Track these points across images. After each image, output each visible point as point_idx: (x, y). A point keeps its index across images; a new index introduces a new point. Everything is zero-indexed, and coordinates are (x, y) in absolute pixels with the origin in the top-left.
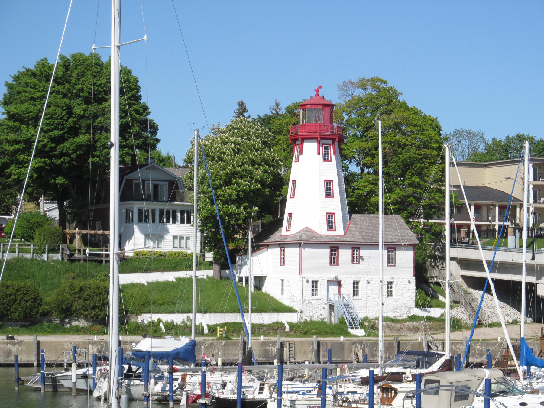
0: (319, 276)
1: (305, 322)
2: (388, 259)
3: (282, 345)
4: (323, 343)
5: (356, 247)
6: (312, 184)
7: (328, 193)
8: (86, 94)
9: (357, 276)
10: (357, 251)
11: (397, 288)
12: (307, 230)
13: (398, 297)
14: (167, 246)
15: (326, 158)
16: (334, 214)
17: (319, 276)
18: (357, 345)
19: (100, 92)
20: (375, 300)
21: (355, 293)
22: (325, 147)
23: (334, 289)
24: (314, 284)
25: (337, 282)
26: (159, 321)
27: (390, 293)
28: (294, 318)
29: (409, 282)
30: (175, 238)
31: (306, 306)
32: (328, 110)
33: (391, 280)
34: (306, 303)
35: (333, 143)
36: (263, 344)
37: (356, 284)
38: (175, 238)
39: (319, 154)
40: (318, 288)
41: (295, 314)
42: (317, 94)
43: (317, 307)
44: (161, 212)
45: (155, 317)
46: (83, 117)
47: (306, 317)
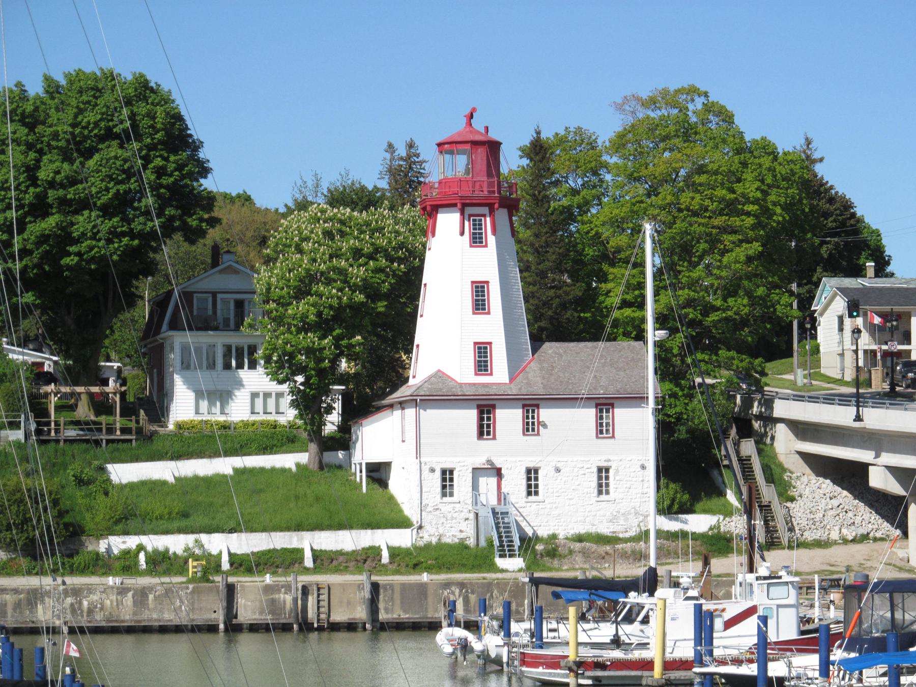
0: (458, 459)
1: (428, 546)
2: (480, 427)
3: (305, 591)
4: (385, 586)
5: (530, 405)
6: (462, 289)
7: (480, 305)
8: (62, 144)
9: (533, 459)
10: (533, 411)
11: (617, 478)
12: (440, 375)
14: (239, 410)
15: (477, 240)
18: (453, 588)
19: (86, 138)
20: (571, 502)
21: (532, 489)
22: (474, 220)
23: (488, 484)
24: (447, 476)
25: (495, 471)
26: (141, 548)
27: (602, 487)
28: (402, 538)
29: (643, 467)
30: (254, 395)
31: (430, 517)
32: (481, 152)
34: (429, 509)
35: (492, 213)
36: (268, 589)
37: (532, 474)
38: (254, 395)
39: (462, 233)
40: (455, 483)
41: (408, 531)
42: (469, 124)
43: (452, 518)
44: (228, 348)
45: (132, 542)
46: (52, 184)
47: (429, 536)
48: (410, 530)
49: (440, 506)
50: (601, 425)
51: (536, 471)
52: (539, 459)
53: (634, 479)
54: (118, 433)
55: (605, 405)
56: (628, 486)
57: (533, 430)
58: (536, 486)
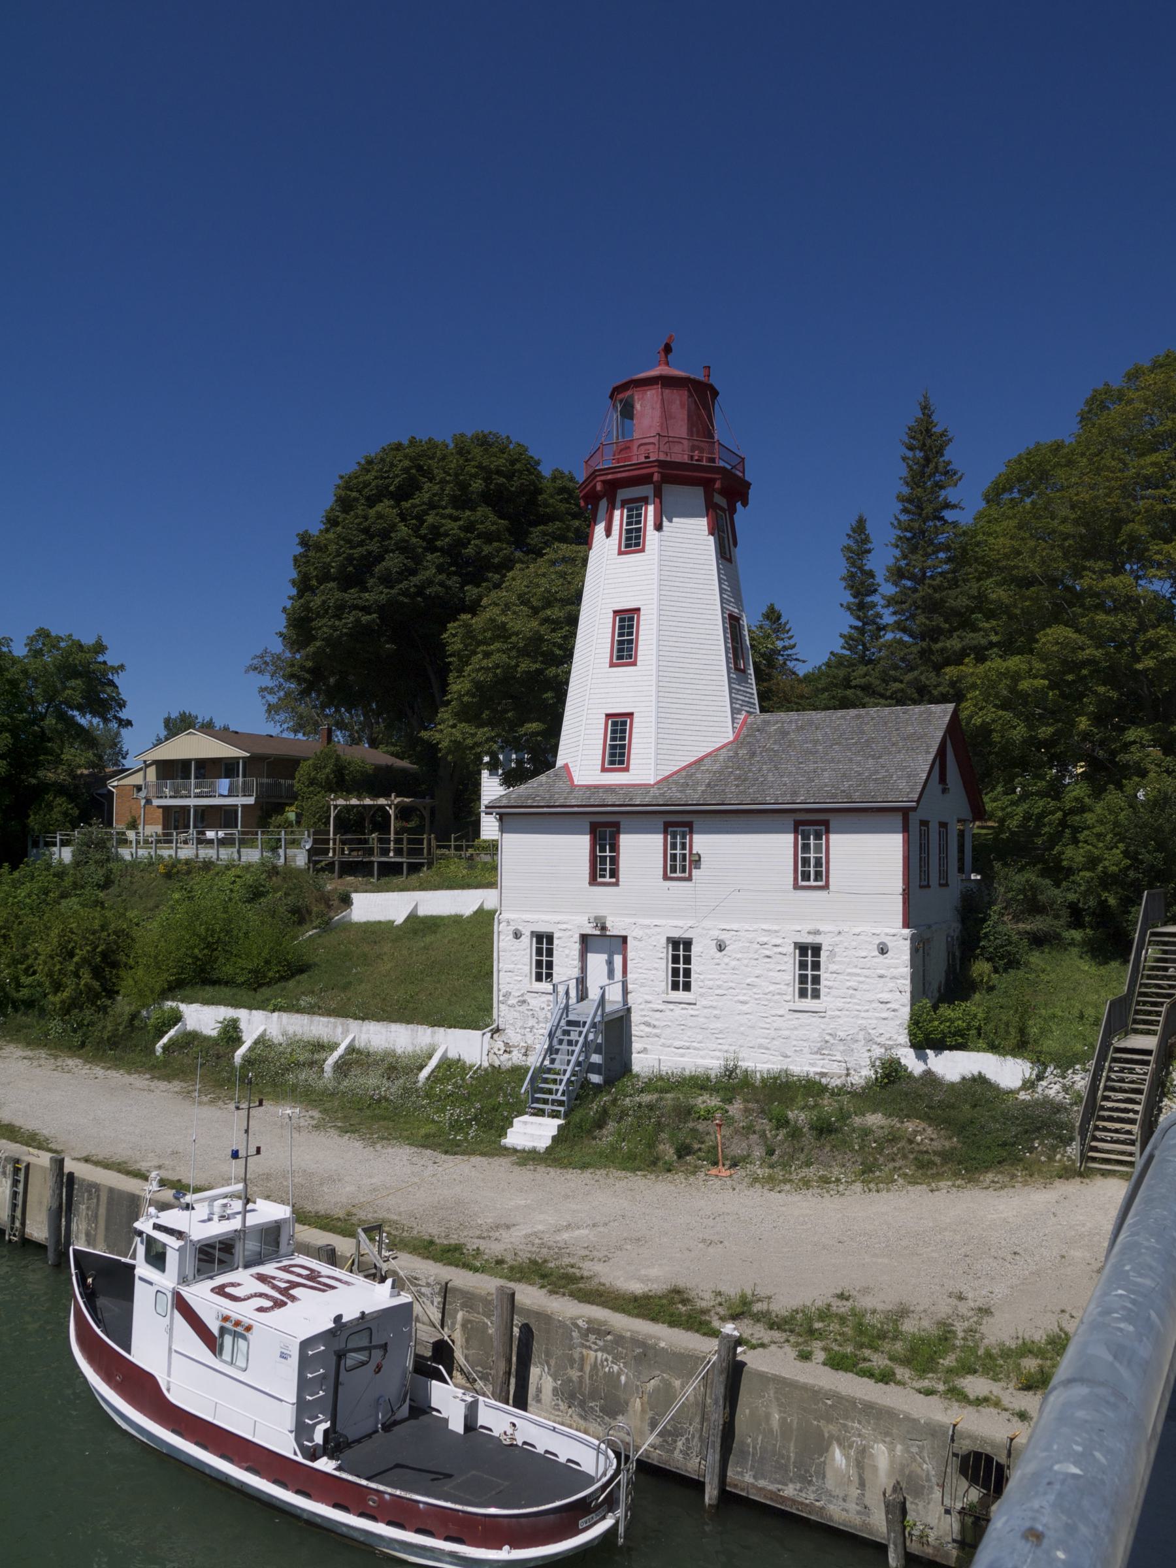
9: (680, 923)
10: (684, 837)
11: (833, 967)
13: (839, 1003)
16: (631, 715)
20: (745, 1008)
21: (681, 979)
33: (809, 939)
35: (658, 494)
48: (480, 1032)
49: (527, 997)
51: (688, 944)
52: (690, 923)
55: (811, 824)
57: (684, 871)
58: (687, 973)
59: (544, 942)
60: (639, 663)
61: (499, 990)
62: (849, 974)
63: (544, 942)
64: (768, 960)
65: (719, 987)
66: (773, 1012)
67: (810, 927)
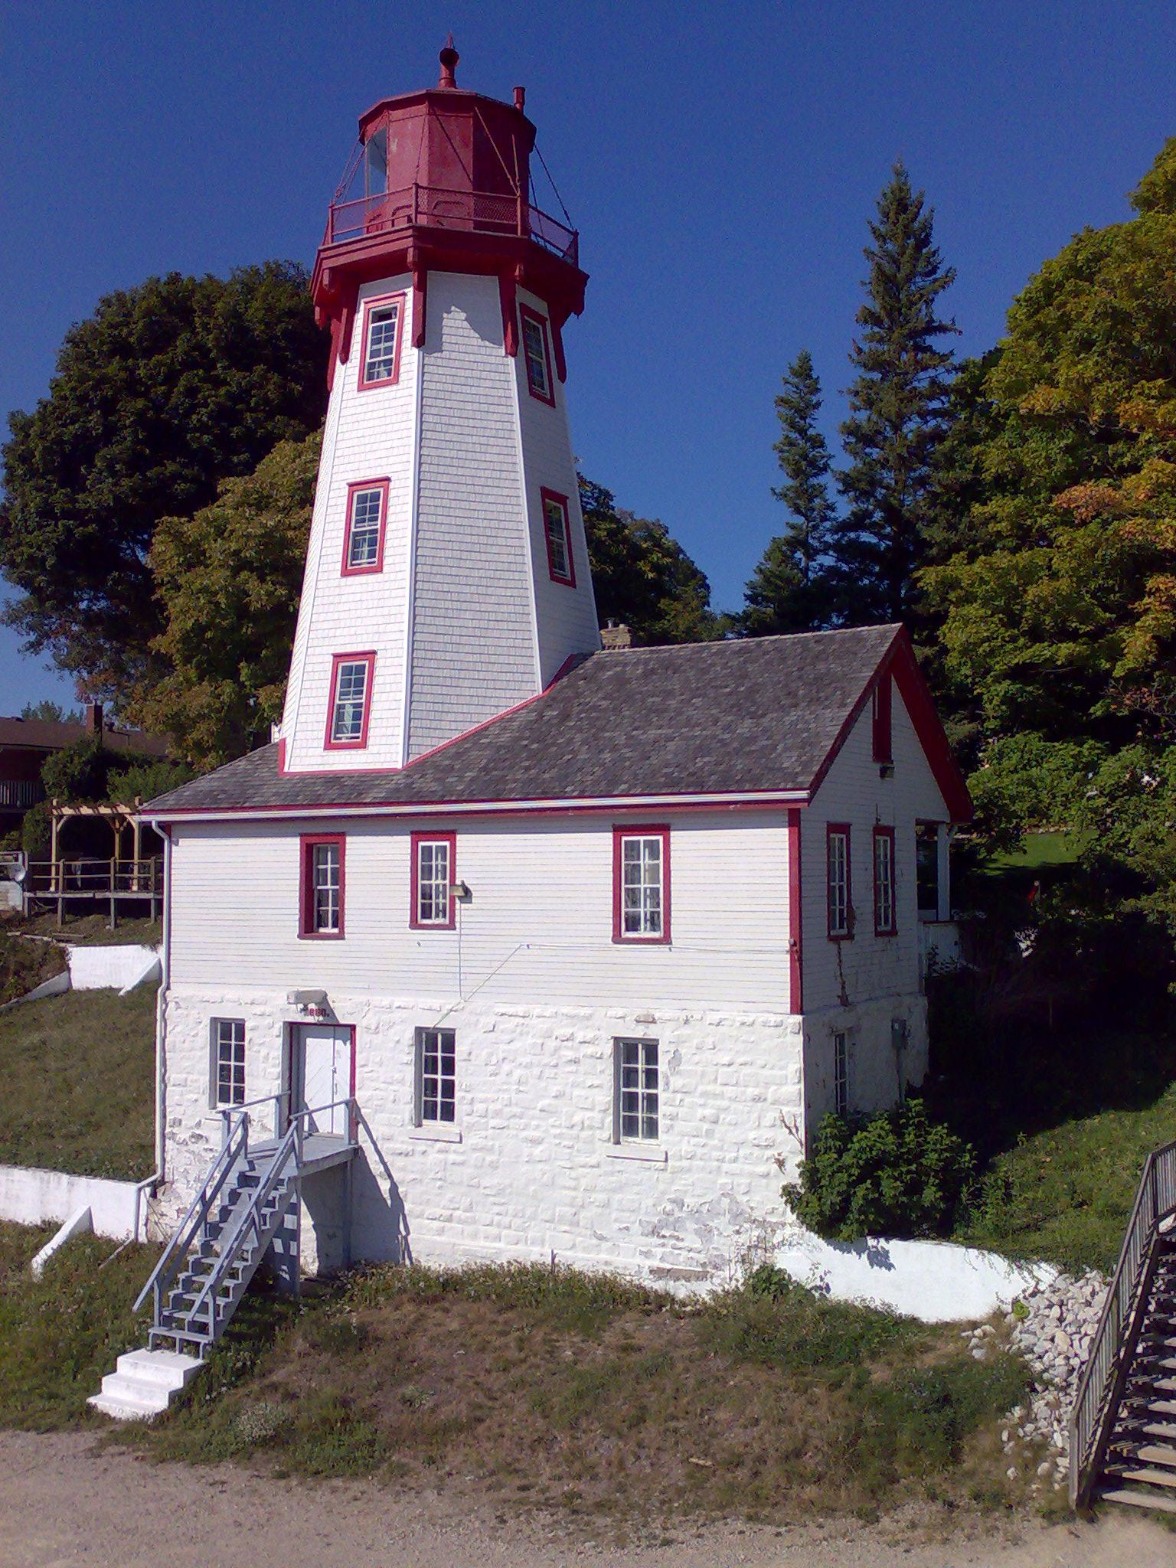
9: (436, 1006)
13: (685, 1148)
17: (257, 994)
20: (537, 1151)
21: (436, 1098)
27: (635, 1108)
33: (638, 1032)
37: (436, 1051)
50: (633, 898)
53: (730, 1091)
54: (135, 888)
55: (640, 829)
56: (708, 1112)
59: (229, 1037)
60: (385, 569)
61: (164, 1116)
62: (704, 1094)
63: (229, 1037)
64: (573, 1068)
65: (498, 1113)
66: (582, 1160)
67: (640, 1012)
